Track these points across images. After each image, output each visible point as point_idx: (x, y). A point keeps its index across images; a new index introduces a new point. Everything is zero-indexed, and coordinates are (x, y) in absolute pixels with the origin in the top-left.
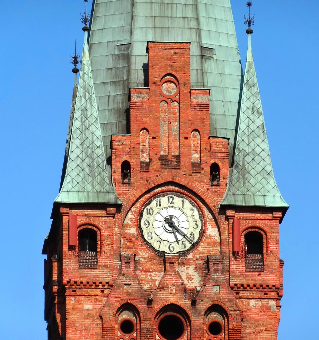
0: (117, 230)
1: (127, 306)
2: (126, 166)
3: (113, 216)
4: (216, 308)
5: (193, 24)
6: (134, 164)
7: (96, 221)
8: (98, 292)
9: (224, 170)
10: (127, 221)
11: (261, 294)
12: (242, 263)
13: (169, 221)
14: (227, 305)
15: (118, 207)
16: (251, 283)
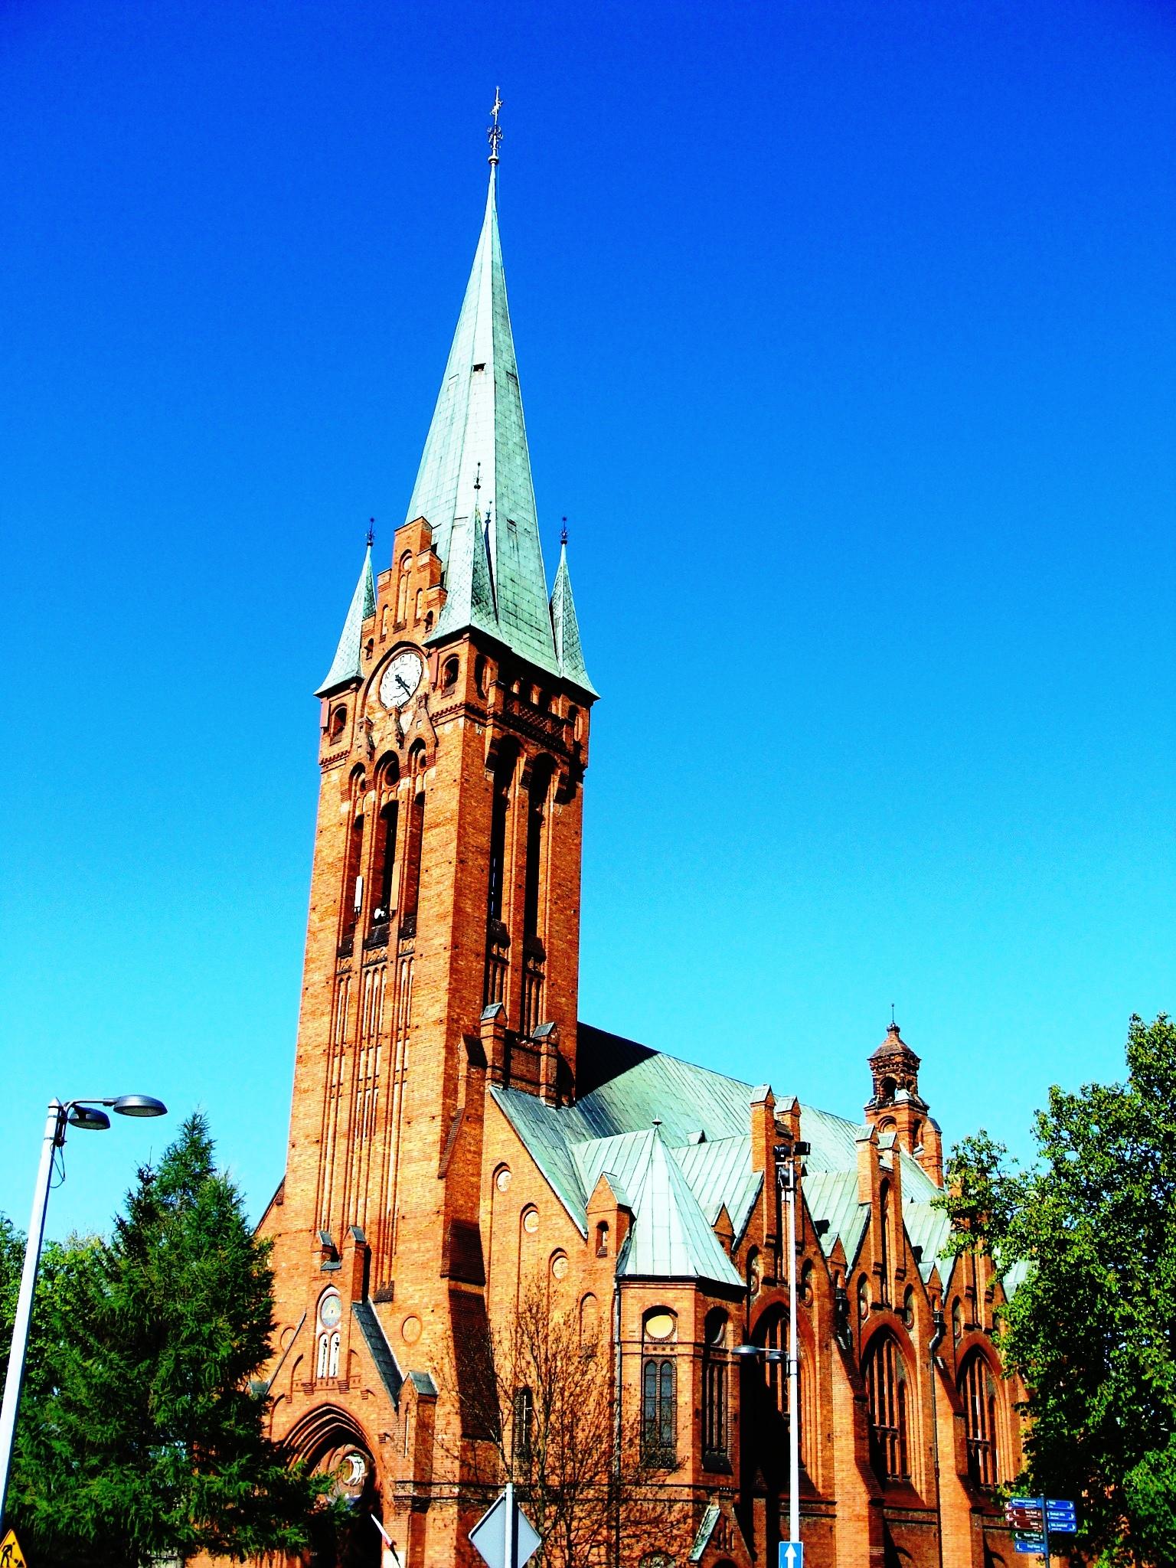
0: (360, 702)
1: (359, 768)
2: (371, 642)
3: (357, 690)
4: (419, 744)
5: (452, 503)
6: (376, 638)
7: (344, 700)
8: (343, 761)
9: (436, 615)
10: (371, 691)
11: (453, 716)
12: (439, 692)
13: (399, 679)
14: (428, 737)
15: (358, 680)
16: (444, 708)
